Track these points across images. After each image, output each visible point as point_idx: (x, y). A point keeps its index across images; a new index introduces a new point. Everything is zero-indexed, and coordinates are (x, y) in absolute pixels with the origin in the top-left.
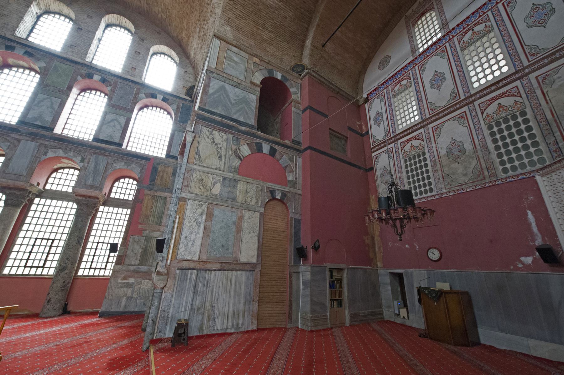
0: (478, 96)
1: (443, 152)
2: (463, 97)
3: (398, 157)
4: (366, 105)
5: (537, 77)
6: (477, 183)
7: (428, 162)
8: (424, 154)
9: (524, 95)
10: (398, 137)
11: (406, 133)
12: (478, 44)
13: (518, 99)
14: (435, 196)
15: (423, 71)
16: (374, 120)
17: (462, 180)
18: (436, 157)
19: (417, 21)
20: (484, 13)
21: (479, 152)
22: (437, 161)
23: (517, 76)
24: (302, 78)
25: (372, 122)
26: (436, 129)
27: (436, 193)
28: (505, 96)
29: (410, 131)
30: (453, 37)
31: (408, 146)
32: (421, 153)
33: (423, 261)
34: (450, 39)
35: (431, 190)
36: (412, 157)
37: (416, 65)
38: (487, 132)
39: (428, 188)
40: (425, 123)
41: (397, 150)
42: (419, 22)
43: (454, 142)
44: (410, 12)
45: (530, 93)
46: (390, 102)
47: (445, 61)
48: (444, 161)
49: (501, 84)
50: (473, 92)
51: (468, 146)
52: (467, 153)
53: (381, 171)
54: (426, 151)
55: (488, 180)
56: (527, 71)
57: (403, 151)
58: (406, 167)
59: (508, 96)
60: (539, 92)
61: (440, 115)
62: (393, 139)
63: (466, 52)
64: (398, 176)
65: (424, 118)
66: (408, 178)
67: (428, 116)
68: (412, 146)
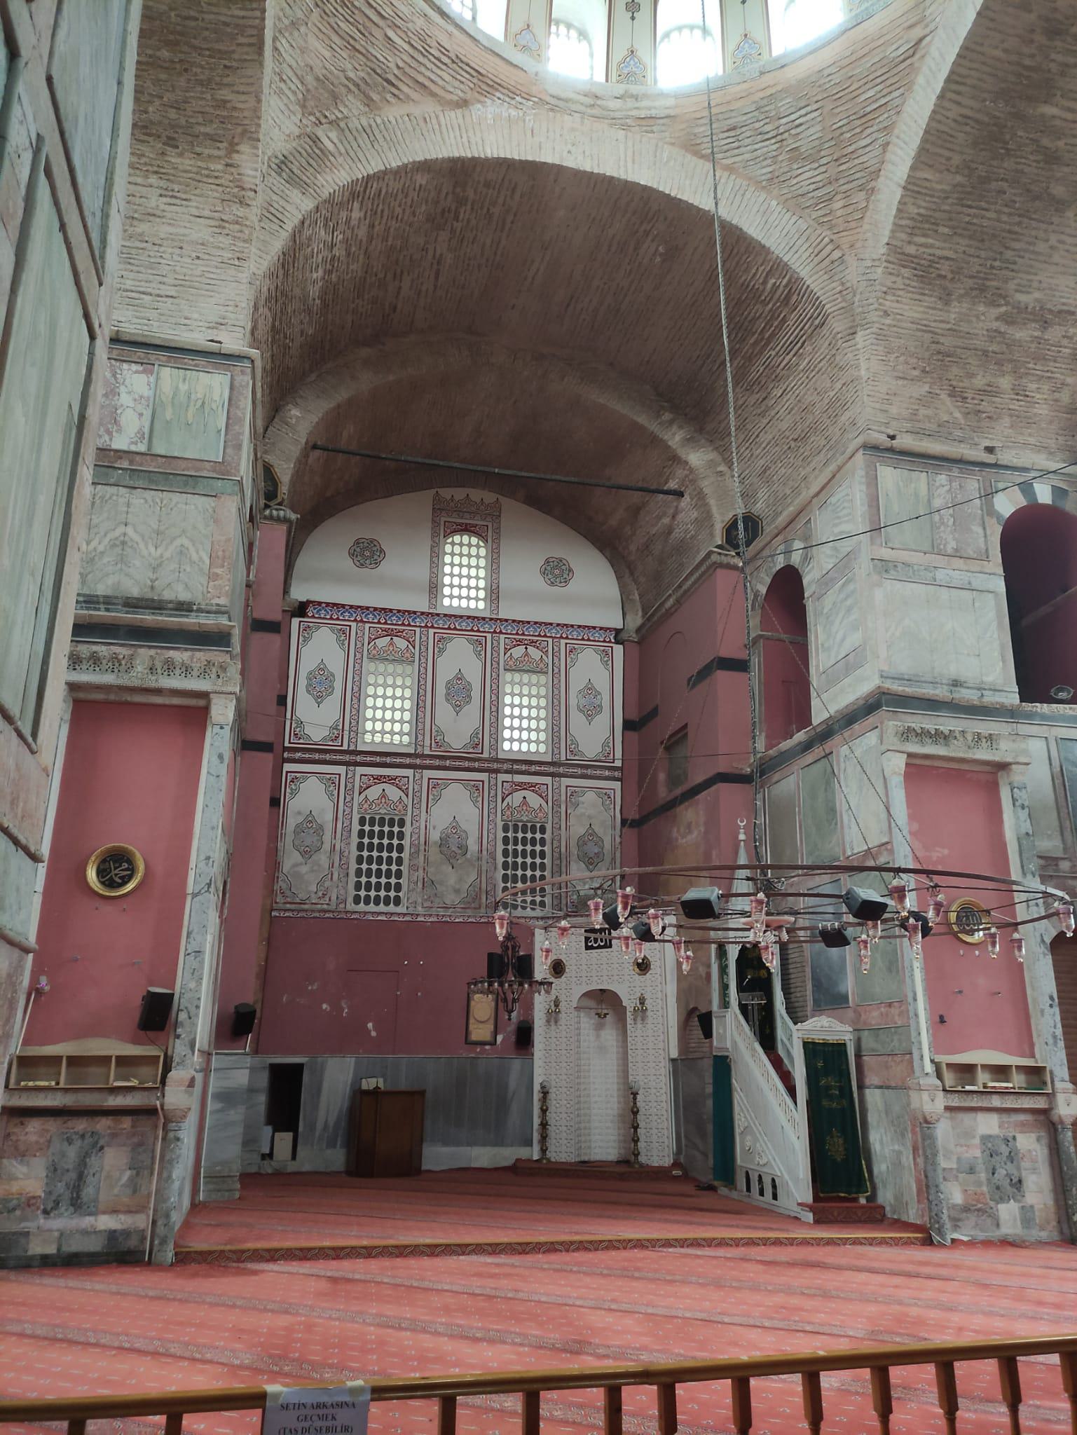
0: (505, 766)
1: (435, 836)
2: (486, 755)
3: (349, 804)
4: (295, 621)
6: (469, 912)
7: (406, 842)
8: (402, 823)
10: (359, 759)
11: (378, 759)
12: (526, 677)
13: (544, 804)
14: (405, 915)
15: (441, 651)
16: (309, 679)
17: (451, 898)
18: (422, 839)
19: (455, 532)
20: (545, 636)
21: (484, 862)
22: (422, 848)
23: (552, 769)
24: (265, 518)
25: (302, 683)
26: (434, 785)
27: (405, 911)
29: (388, 760)
30: (501, 632)
31: (374, 792)
32: (397, 819)
33: (344, 1038)
34: (495, 632)
35: (397, 901)
36: (377, 817)
37: (432, 627)
38: (501, 834)
39: (392, 894)
40: (418, 761)
41: (350, 786)
42: (457, 539)
43: (455, 825)
44: (446, 493)
45: (556, 804)
46: (359, 662)
48: (434, 854)
49: (533, 768)
51: (473, 846)
52: (468, 855)
53: (300, 819)
54: (408, 820)
55: (483, 910)
56: (561, 770)
57: (363, 796)
58: (361, 834)
59: (536, 792)
60: (563, 807)
61: (448, 763)
62: (347, 758)
63: (508, 676)
64: (338, 848)
65: (419, 750)
66: (360, 860)
67: (427, 752)
68: (384, 795)
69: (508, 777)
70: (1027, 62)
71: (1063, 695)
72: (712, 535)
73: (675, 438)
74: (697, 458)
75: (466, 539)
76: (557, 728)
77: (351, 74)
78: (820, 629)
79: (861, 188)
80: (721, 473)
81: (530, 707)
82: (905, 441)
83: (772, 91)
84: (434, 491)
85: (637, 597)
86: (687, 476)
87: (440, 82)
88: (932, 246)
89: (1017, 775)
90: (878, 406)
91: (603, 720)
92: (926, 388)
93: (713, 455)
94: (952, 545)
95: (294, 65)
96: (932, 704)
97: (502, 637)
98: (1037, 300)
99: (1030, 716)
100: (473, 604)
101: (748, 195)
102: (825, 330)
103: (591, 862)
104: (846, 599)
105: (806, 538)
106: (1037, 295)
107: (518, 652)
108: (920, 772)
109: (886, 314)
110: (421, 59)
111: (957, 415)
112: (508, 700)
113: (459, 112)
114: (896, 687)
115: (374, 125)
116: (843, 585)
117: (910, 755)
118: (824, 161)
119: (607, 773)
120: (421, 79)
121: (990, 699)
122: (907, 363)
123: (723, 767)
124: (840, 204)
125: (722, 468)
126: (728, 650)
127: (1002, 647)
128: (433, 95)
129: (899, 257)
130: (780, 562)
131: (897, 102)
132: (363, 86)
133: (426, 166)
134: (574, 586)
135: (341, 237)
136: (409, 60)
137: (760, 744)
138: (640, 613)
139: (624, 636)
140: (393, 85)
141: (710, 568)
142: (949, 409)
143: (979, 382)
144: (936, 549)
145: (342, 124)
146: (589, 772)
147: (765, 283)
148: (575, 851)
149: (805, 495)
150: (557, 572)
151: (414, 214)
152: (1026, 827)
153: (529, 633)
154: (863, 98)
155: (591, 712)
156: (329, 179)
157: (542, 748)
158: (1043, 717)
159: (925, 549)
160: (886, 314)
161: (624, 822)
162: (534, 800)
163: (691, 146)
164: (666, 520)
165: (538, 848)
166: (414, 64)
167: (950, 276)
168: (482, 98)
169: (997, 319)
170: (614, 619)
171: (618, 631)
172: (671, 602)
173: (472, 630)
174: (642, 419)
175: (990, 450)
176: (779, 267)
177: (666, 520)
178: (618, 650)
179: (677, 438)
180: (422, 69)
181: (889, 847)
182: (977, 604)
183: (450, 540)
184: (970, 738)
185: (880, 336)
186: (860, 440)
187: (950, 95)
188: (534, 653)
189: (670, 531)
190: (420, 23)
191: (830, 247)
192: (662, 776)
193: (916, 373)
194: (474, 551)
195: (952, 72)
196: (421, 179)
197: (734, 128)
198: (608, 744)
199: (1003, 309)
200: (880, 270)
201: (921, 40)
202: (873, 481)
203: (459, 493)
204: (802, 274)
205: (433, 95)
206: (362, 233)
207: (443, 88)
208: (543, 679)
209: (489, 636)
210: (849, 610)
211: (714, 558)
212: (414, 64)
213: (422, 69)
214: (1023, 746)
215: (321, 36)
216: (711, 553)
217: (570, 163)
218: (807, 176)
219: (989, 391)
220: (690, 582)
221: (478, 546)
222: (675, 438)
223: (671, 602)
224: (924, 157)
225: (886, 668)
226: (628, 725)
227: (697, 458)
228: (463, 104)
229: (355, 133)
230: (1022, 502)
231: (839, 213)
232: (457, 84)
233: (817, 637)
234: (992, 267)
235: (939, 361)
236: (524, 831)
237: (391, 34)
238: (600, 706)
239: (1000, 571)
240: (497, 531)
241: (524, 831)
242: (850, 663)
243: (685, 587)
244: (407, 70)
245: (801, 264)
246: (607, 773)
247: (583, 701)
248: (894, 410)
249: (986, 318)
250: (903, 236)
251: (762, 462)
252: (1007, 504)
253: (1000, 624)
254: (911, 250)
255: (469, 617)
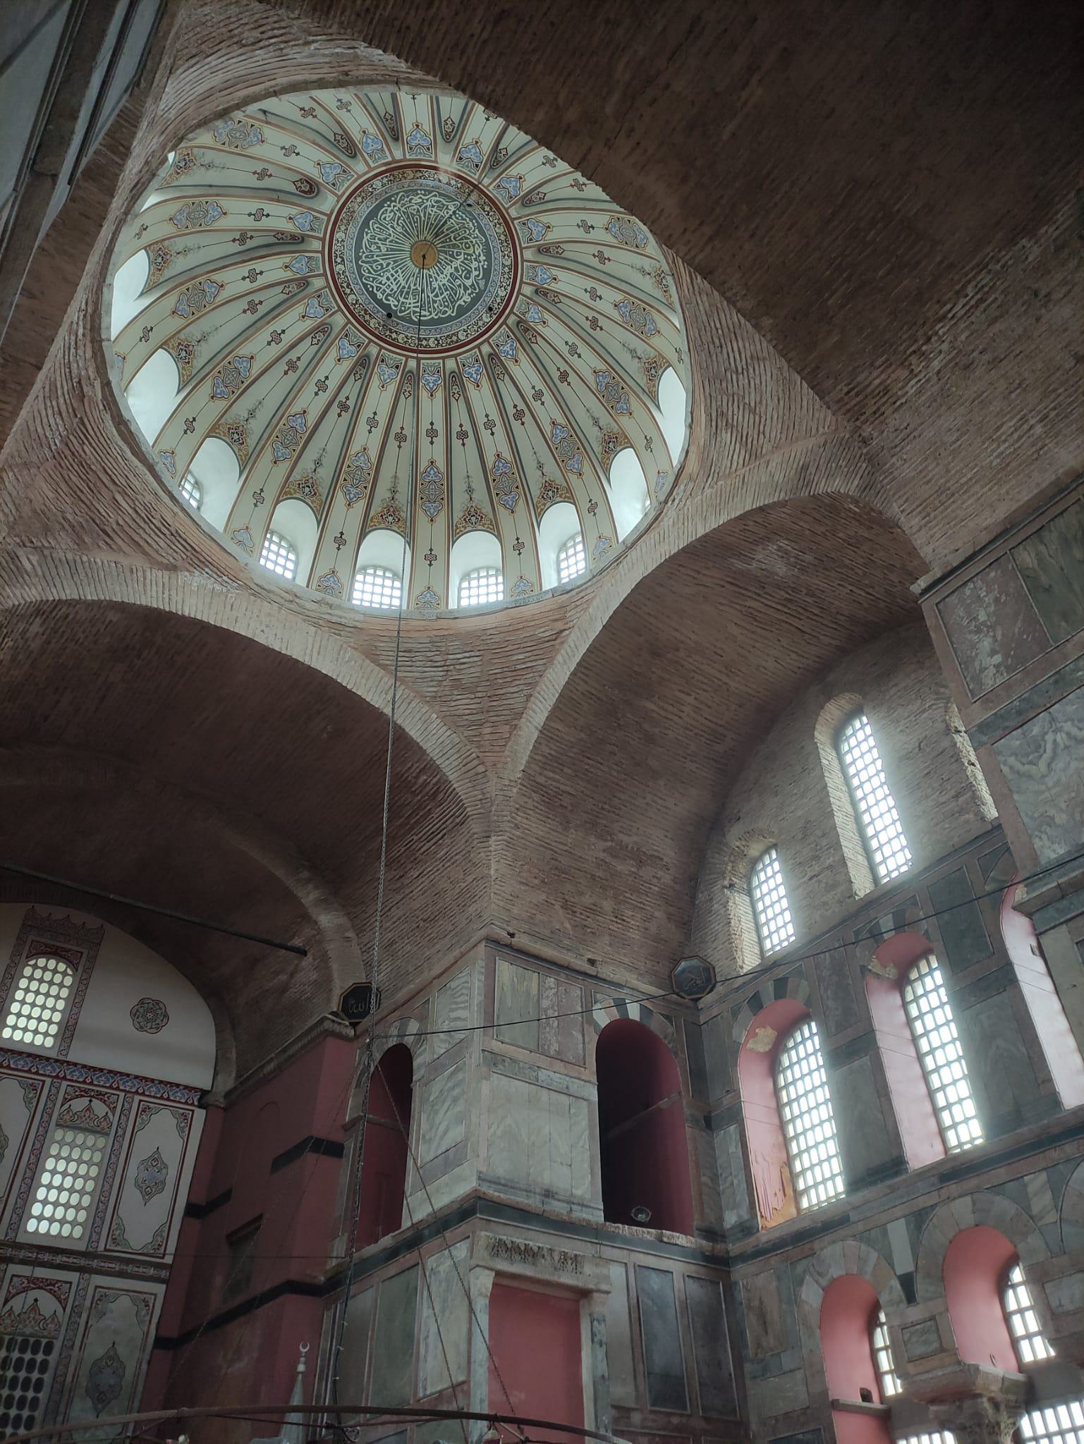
5: (96, 1287)
9: (68, 1309)
12: (80, 1138)
20: (117, 1089)
23: (82, 1262)
28: (50, 1291)
30: (64, 1078)
34: (57, 1077)
42: (42, 962)
44: (43, 910)
45: (76, 1311)
47: (26, 1114)
49: (60, 1259)
50: (21, 1239)
56: (95, 1263)
60: (84, 1316)
63: (59, 1134)
69: (25, 1270)
70: (636, 669)
71: (641, 1217)
72: (329, 1000)
73: (309, 896)
74: (327, 920)
75: (52, 963)
76: (104, 1207)
77: (69, 517)
78: (424, 1117)
79: (507, 722)
80: (348, 939)
81: (75, 1176)
82: (522, 940)
83: (442, 633)
84: (28, 906)
85: (234, 1055)
86: (314, 936)
87: (155, 546)
88: (558, 781)
89: (599, 1306)
90: (501, 904)
91: (161, 1202)
92: (544, 898)
93: (343, 920)
94: (555, 1047)
95: (14, 493)
96: (523, 1215)
97: (65, 1083)
98: (635, 843)
99: (613, 1237)
100: (39, 1040)
101: (414, 704)
102: (464, 828)
103: (101, 1398)
104: (453, 1088)
105: (423, 1018)
106: (635, 838)
107: (79, 1104)
108: (508, 1293)
109: (517, 827)
110: (142, 524)
111: (568, 926)
112: (50, 1164)
113: (166, 573)
114: (492, 1192)
115: (79, 561)
116: (453, 1073)
117: (499, 1274)
118: (479, 695)
119: (152, 1271)
120: (137, 538)
121: (580, 1214)
122: (529, 871)
123: (294, 1272)
124: (489, 730)
125: (350, 934)
126: (322, 1128)
127: (592, 1157)
128: (145, 553)
129: (531, 782)
130: (392, 1042)
131: (540, 668)
132: (78, 528)
133: (122, 607)
134: (168, 1035)
135: (11, 644)
136: (131, 522)
137: (339, 1247)
138: (233, 1075)
139: (210, 1099)
140: (109, 536)
141: (319, 1035)
142: (561, 920)
143: (587, 900)
144: (540, 1049)
145: (47, 552)
146: (130, 1268)
147: (417, 777)
148: (83, 1381)
149: (427, 975)
150: (150, 1016)
151: (95, 643)
152: (603, 1368)
153: (98, 1083)
154: (515, 658)
155: (149, 1190)
156: (17, 593)
157: (78, 1232)
158: (626, 1241)
159: (532, 1048)
160: (517, 827)
161: (160, 1342)
162: (48, 1304)
163: (372, 654)
164: (283, 977)
165: (35, 1375)
166: (134, 526)
167: (570, 808)
168: (191, 569)
169: (604, 851)
170: (203, 1079)
171: (204, 1093)
172: (272, 1066)
173: (29, 1071)
174: (280, 873)
175: (592, 962)
176: (431, 767)
177: (283, 977)
178: (200, 1115)
179: (311, 897)
180: (141, 532)
181: (465, 1387)
182: (573, 1111)
183: (32, 962)
184: (556, 1258)
185: (509, 844)
186: (483, 932)
187: (580, 674)
188: (99, 1108)
189: (284, 989)
190: (149, 498)
191: (476, 762)
192: (219, 1280)
193: (536, 881)
194: (58, 978)
195: (583, 659)
196: (113, 616)
197: (410, 651)
198: (162, 1234)
199: (609, 844)
200: (515, 790)
201: (562, 631)
202: (491, 974)
203: (59, 913)
204: (451, 778)
205: (145, 553)
206: (34, 646)
207: (157, 551)
208: (101, 1142)
209: (48, 1080)
210: (455, 1100)
211: (327, 1025)
212: (134, 526)
213: (141, 532)
214: (605, 1271)
215: (49, 480)
216: (325, 1019)
217: (261, 639)
218: (464, 703)
219: (593, 910)
220: (296, 1047)
221: (64, 974)
222: (309, 896)
223: (272, 1066)
224: (556, 713)
225: (484, 1169)
226: (192, 1210)
227: (327, 920)
228: (173, 568)
229: (57, 562)
230: (615, 1014)
231: (487, 737)
232: (170, 551)
233: (419, 1126)
234: (603, 809)
235: (555, 875)
236: (23, 1350)
237: (119, 497)
238: (164, 1183)
239: (594, 1079)
240: (92, 960)
241: (23, 1350)
242: (451, 1159)
243: (291, 1052)
244: (127, 528)
245: (450, 767)
246: (152, 1271)
247: (144, 1175)
248: (515, 911)
249: (595, 849)
250: (537, 768)
251: (390, 935)
252: (603, 1018)
253: (591, 1136)
254: (541, 780)
255: (29, 1055)
